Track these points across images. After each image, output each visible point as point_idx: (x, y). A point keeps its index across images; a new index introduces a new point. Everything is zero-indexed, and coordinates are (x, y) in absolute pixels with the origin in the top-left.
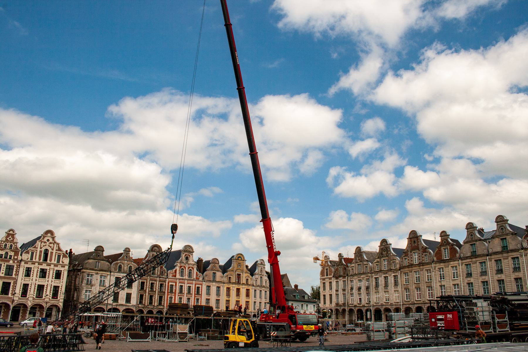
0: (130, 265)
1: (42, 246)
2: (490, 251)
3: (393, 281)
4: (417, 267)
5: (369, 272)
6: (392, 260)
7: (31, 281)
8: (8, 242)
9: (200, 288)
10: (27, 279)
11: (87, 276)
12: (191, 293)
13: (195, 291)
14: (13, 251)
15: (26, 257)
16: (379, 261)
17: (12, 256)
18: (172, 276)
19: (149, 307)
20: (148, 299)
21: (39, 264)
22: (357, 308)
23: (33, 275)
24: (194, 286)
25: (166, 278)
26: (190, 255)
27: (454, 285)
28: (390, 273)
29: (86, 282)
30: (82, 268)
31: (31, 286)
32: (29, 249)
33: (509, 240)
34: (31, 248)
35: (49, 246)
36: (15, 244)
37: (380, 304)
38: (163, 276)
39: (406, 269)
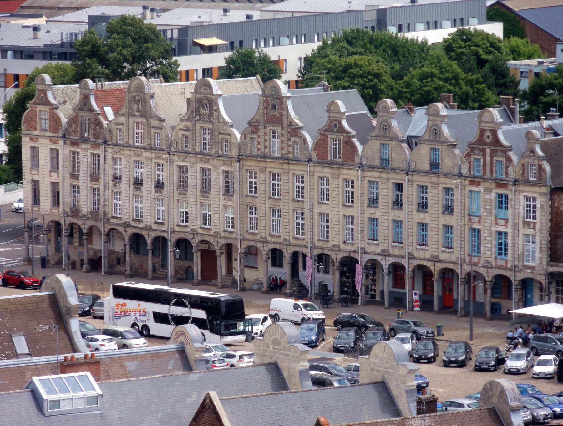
2: (413, 167)
3: (222, 184)
4: (277, 164)
5: (164, 147)
16: (191, 129)
22: (130, 231)
27: (347, 217)
33: (444, 154)
37: (188, 230)
39: (253, 163)
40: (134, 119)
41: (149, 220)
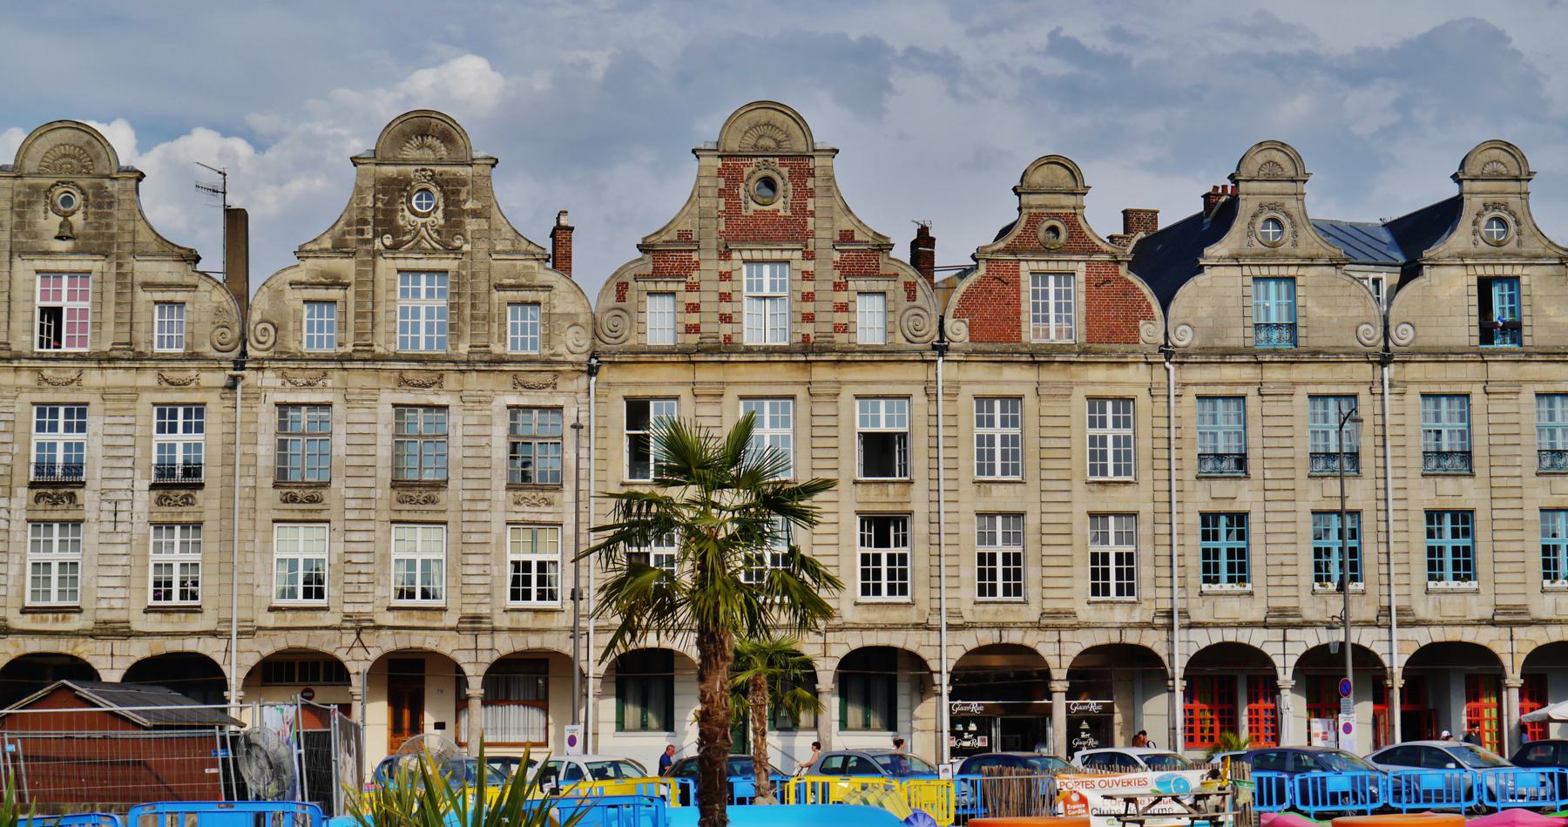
2: (1403, 336)
5: (207, 349)
6: (501, 287)
16: (351, 277)
28: (359, 380)
33: (1537, 292)
40: (41, 264)
41: (117, 603)
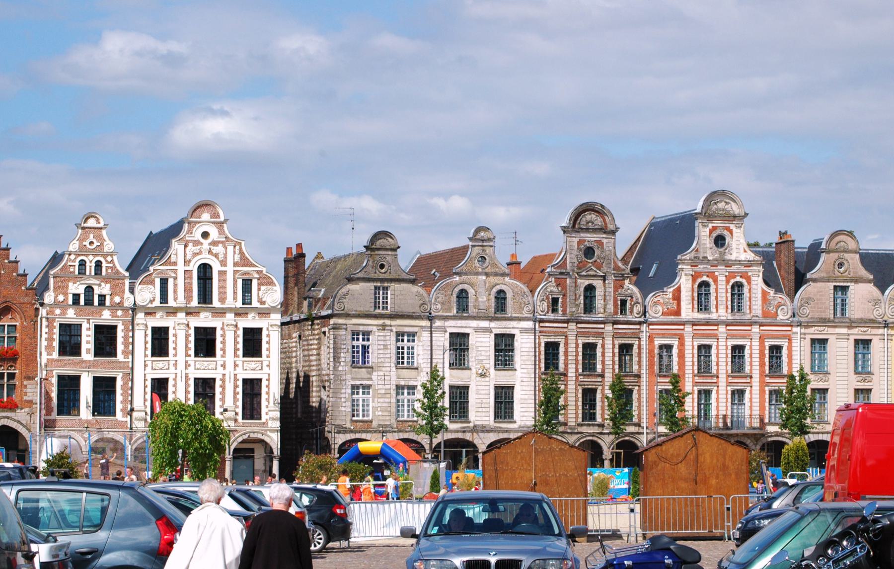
0: (498, 287)
1: (189, 257)
7: (172, 368)
8: (87, 255)
9: (785, 352)
10: (160, 362)
11: (350, 337)
12: (747, 369)
13: (762, 365)
14: (107, 280)
15: (147, 294)
17: (104, 296)
18: (663, 314)
19: (584, 429)
20: (576, 401)
21: (188, 314)
23: (175, 349)
24: (756, 344)
25: (640, 323)
26: (732, 227)
29: (349, 359)
30: (330, 312)
31: (175, 386)
32: (151, 269)
34: (156, 267)
35: (210, 252)
36: (109, 259)
38: (630, 318)
